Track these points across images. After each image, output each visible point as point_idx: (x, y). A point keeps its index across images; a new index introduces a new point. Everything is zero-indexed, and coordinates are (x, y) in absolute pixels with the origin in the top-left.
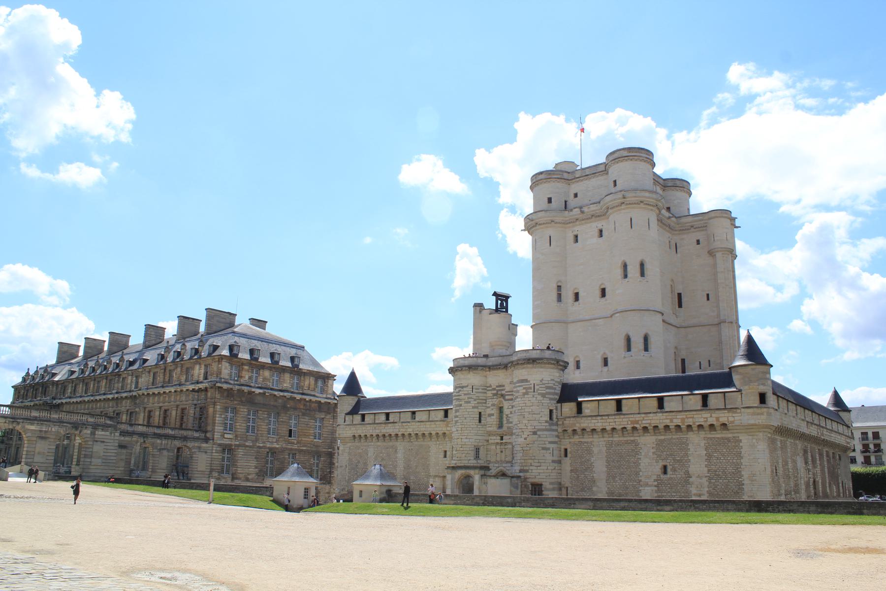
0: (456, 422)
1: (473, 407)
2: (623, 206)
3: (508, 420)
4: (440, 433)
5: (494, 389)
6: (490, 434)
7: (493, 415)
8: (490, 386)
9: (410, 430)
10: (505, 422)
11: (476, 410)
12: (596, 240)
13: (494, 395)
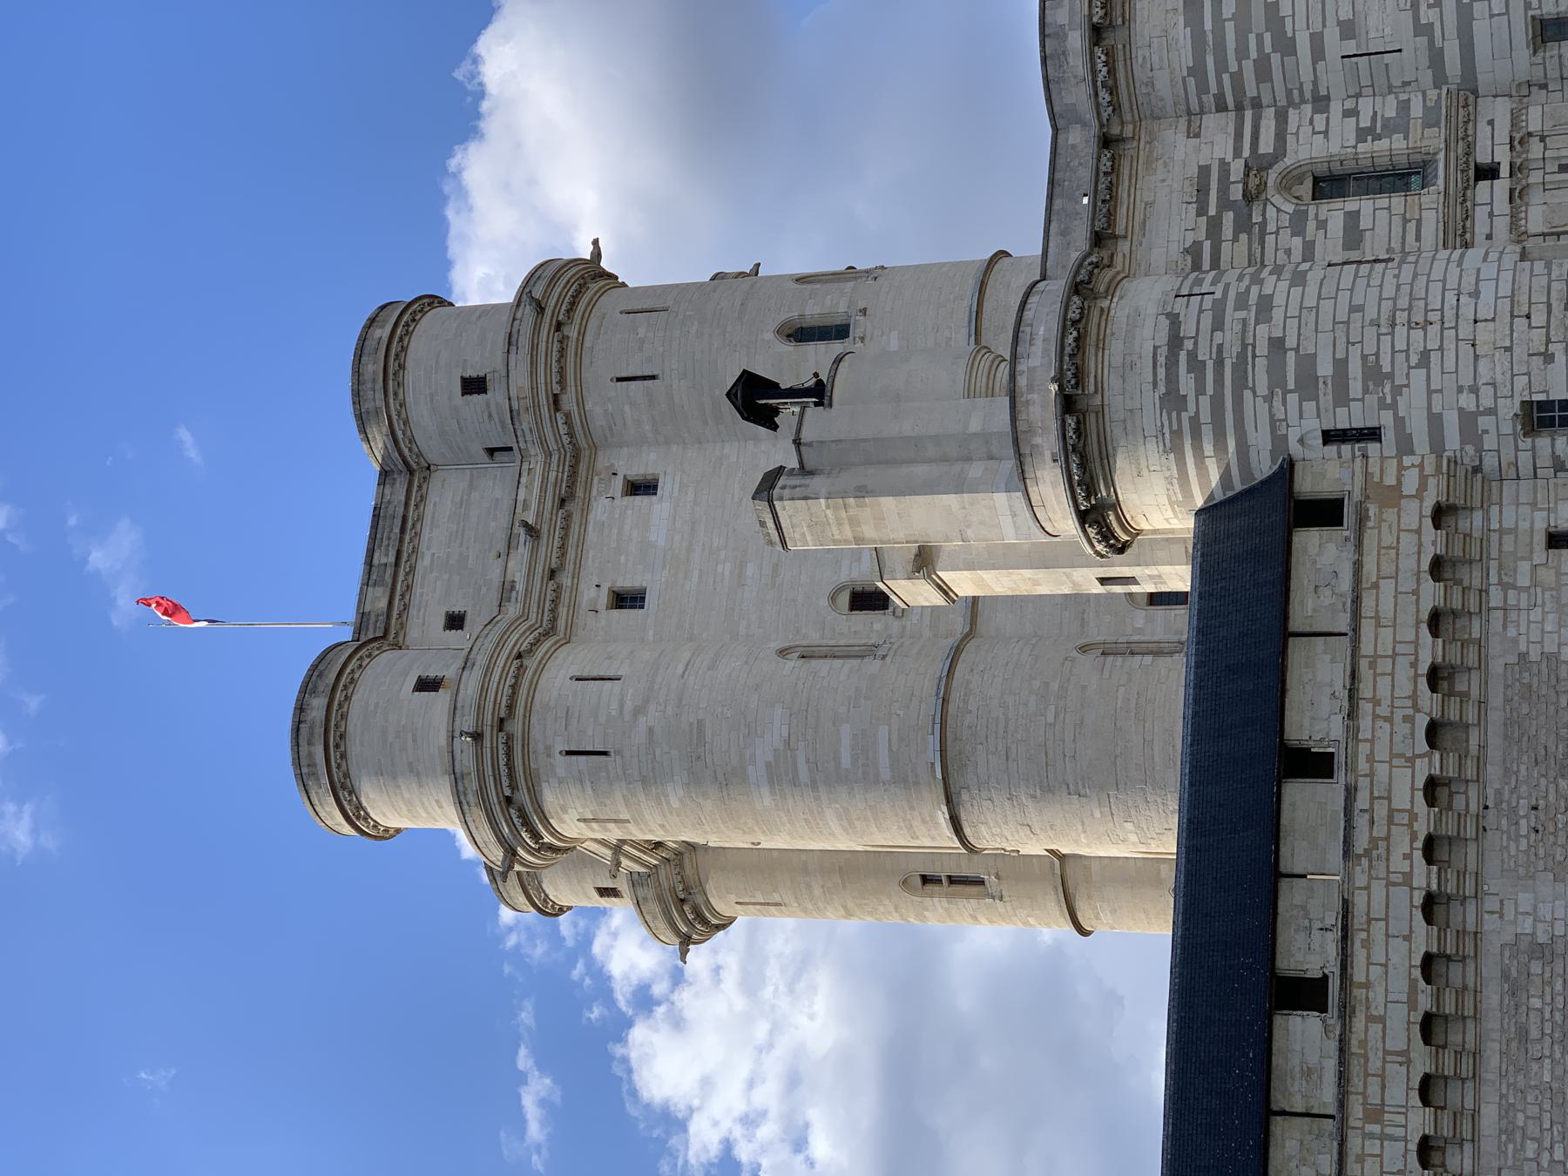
0: (1374, 374)
1: (1299, 279)
2: (572, 332)
3: (1390, 128)
4: (1433, 542)
5: (1214, 227)
6: (1458, 235)
7: (1353, 218)
8: (1194, 251)
9: (1406, 788)
10: (1398, 143)
11: (1313, 278)
12: (657, 508)
13: (1243, 225)
